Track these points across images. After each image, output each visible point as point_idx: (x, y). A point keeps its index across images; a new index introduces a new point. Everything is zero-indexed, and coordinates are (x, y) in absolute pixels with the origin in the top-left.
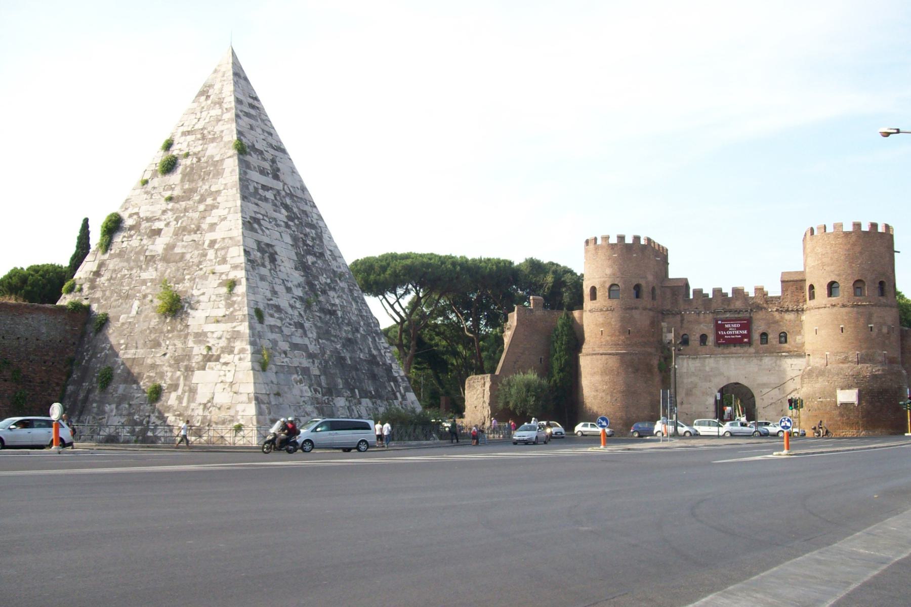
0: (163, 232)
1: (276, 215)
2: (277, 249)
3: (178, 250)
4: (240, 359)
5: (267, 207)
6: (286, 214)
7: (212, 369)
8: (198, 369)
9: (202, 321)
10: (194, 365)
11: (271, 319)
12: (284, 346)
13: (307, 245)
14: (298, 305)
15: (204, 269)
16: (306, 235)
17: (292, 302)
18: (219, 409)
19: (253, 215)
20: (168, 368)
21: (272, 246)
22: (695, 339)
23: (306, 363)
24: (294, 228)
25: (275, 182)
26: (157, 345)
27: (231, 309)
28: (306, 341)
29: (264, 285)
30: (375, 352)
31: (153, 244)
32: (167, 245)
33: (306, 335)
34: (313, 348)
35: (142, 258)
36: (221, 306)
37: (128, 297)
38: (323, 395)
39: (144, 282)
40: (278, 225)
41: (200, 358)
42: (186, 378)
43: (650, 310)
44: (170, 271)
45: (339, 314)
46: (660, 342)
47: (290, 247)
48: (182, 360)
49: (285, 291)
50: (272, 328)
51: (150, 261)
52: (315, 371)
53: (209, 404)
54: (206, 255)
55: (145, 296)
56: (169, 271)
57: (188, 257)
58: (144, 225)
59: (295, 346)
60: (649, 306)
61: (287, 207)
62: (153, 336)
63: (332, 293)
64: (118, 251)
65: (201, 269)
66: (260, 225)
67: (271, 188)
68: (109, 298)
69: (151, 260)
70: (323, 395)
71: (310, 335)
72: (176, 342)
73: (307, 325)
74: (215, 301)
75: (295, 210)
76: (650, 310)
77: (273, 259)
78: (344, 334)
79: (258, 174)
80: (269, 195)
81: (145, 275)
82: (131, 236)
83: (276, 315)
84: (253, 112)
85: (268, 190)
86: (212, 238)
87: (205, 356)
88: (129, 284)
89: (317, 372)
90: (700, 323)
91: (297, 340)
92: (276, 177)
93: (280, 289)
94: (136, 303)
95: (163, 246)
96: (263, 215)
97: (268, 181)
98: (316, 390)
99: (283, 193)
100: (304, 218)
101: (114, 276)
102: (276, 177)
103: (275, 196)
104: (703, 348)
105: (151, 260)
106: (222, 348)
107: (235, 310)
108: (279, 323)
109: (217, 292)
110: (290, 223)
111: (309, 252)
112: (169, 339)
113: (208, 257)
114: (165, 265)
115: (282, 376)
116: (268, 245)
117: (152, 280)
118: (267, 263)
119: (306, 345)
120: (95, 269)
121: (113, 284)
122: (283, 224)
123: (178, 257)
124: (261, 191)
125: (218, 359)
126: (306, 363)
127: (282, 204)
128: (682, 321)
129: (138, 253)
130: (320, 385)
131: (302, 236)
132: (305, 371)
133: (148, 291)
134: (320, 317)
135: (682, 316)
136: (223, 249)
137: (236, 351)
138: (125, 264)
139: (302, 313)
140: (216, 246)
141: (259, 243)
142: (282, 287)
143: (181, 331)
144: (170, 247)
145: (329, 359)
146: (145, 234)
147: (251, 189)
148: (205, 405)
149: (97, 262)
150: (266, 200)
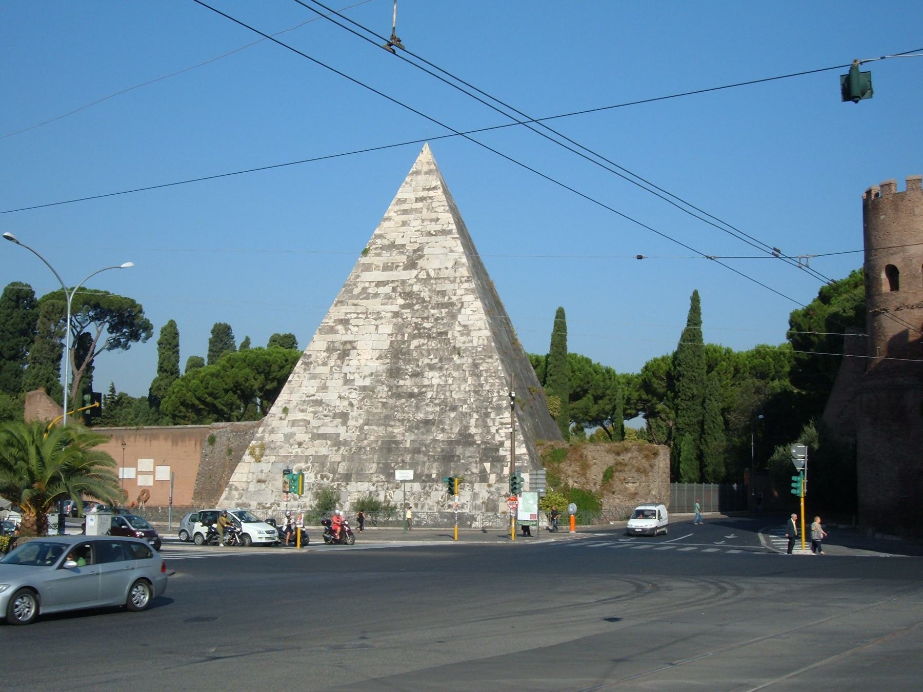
16: (427, 318)
21: (351, 342)
30: (473, 430)
38: (333, 481)
45: (429, 395)
50: (294, 423)
61: (408, 295)
63: (431, 374)
67: (393, 281)
70: (333, 481)
71: (351, 423)
73: (354, 413)
78: (421, 416)
80: (388, 289)
83: (311, 409)
84: (420, 205)
89: (338, 459)
93: (336, 385)
98: (322, 477)
108: (309, 417)
119: (338, 435)
126: (323, 451)
130: (334, 472)
139: (355, 402)
145: (369, 445)
147: (356, 291)
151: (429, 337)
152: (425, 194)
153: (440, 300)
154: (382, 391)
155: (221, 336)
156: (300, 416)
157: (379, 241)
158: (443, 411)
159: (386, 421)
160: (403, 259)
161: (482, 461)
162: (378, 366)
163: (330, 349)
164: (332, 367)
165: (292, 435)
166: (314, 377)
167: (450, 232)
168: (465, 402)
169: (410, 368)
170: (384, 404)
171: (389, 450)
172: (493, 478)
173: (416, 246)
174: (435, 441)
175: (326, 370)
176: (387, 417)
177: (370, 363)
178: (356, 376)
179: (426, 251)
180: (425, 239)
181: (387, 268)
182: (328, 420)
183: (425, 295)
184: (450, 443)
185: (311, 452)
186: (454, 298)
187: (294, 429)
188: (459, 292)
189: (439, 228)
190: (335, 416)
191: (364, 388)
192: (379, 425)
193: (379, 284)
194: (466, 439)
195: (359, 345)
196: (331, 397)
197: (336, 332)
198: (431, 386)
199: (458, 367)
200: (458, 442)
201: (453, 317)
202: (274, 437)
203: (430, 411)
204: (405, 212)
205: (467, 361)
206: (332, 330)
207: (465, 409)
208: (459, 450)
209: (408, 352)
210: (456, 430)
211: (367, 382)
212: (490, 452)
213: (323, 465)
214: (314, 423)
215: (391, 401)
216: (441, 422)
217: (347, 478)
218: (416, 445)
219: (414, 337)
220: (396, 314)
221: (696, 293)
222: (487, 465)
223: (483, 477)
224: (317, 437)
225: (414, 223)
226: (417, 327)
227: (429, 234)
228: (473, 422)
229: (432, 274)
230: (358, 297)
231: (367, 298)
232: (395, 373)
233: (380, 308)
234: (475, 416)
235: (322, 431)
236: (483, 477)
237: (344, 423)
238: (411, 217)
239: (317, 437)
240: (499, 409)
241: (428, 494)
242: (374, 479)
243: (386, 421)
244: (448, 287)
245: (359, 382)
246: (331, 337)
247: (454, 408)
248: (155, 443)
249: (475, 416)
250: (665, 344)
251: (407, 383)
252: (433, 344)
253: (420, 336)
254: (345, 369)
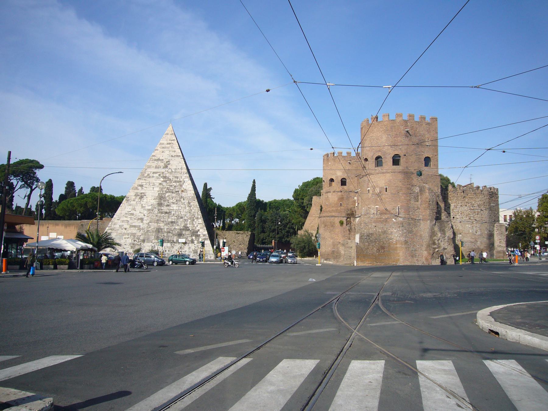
19: (141, 184)
30: (188, 225)
45: (173, 213)
50: (123, 221)
61: (165, 177)
63: (173, 205)
71: (144, 222)
73: (145, 218)
78: (170, 220)
80: (157, 175)
84: (168, 146)
93: (139, 208)
108: (129, 219)
126: (134, 231)
132: (134, 235)
134: (156, 216)
147: (146, 175)
150: (153, 177)
151: (172, 193)
152: (170, 142)
153: (176, 180)
154: (156, 211)
155: (70, 185)
156: (126, 219)
157: (154, 158)
158: (178, 219)
159: (158, 221)
160: (162, 165)
161: (192, 236)
162: (155, 202)
163: (136, 195)
165: (123, 225)
166: (130, 205)
167: (180, 156)
168: (186, 215)
169: (166, 203)
170: (156, 216)
171: (159, 232)
172: (196, 242)
173: (167, 160)
174: (175, 229)
175: (134, 203)
176: (158, 220)
177: (151, 201)
178: (146, 205)
179: (171, 162)
180: (171, 158)
181: (156, 167)
182: (136, 220)
183: (171, 177)
184: (181, 229)
185: (130, 232)
186: (181, 180)
187: (123, 224)
188: (183, 177)
189: (175, 154)
190: (138, 219)
191: (149, 210)
192: (154, 223)
193: (154, 173)
194: (186, 228)
195: (147, 194)
196: (137, 213)
197: (138, 189)
198: (173, 210)
199: (183, 204)
200: (183, 229)
201: (181, 186)
202: (115, 226)
203: (173, 219)
204: (163, 148)
205: (186, 202)
206: (137, 189)
207: (186, 218)
208: (184, 232)
209: (165, 198)
210: (183, 225)
211: (150, 208)
212: (195, 233)
213: (134, 236)
214: (131, 221)
215: (159, 215)
216: (177, 222)
217: (144, 241)
218: (168, 230)
219: (167, 192)
220: (160, 184)
221: (254, 180)
222: (194, 238)
223: (192, 242)
224: (131, 226)
225: (166, 152)
226: (168, 188)
227: (172, 156)
228: (188, 223)
229: (173, 170)
230: (146, 177)
231: (150, 178)
232: (160, 204)
233: (154, 181)
234: (189, 221)
235: (134, 224)
236: (192, 242)
237: (142, 222)
238: (165, 150)
239: (131, 226)
240: (197, 218)
241: (173, 247)
242: (153, 241)
243: (158, 221)
244: (179, 175)
245: (147, 208)
246: (136, 191)
247: (182, 218)
248: (57, 227)
250: (243, 198)
251: (165, 209)
252: (174, 195)
253: (169, 192)
254: (142, 203)
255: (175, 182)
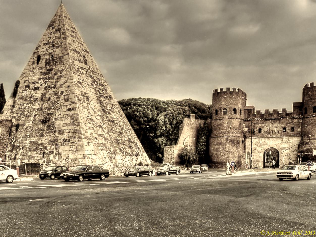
0: (40, 88)
1: (87, 80)
2: (89, 95)
3: (47, 96)
4: (78, 141)
5: (84, 77)
6: (91, 80)
7: (67, 145)
8: (61, 145)
9: (61, 125)
10: (59, 143)
11: (89, 124)
12: (95, 135)
13: (101, 93)
14: (99, 118)
15: (60, 104)
16: (100, 89)
17: (97, 117)
18: (72, 161)
20: (48, 145)
21: (87, 94)
22: (257, 130)
23: (104, 142)
24: (95, 86)
25: (86, 66)
26: (42, 135)
27: (73, 120)
28: (103, 133)
29: (85, 110)
30: (130, 137)
31: (36, 93)
32: (42, 94)
33: (103, 131)
34: (107, 136)
35: (32, 99)
36: (68, 119)
37: (27, 116)
39: (34, 109)
40: (88, 85)
41: (62, 141)
42: (56, 149)
43: (239, 119)
44: (45, 105)
46: (243, 132)
47: (94, 94)
48: (54, 142)
49: (94, 113)
51: (36, 100)
52: (108, 145)
53: (67, 159)
54: (60, 98)
55: (35, 115)
56: (44, 105)
57: (52, 99)
58: (32, 86)
59: (100, 135)
60: (239, 118)
61: (91, 76)
62: (41, 132)
64: (21, 97)
65: (58, 104)
66: (81, 85)
67: (84, 69)
68: (20, 116)
69: (36, 100)
72: (51, 134)
74: (65, 117)
75: (95, 78)
76: (239, 119)
77: (88, 100)
79: (78, 62)
80: (84, 71)
81: (34, 107)
82: (26, 90)
83: (91, 122)
85: (83, 69)
86: (62, 91)
87: (64, 140)
88: (28, 111)
90: (258, 124)
91: (100, 133)
92: (86, 64)
93: (92, 112)
94: (32, 119)
95: (40, 94)
96: (82, 80)
97: (83, 65)
98: (109, 153)
99: (89, 71)
100: (99, 82)
101: (21, 107)
102: (86, 64)
103: (86, 72)
104: (260, 134)
105: (36, 100)
106: (70, 136)
107: (74, 121)
108: (92, 126)
109: (66, 114)
110: (93, 84)
111: (101, 96)
112: (47, 133)
113: (61, 99)
114: (42, 102)
115: (95, 147)
116: (85, 93)
117: (38, 109)
118: (86, 101)
120: (12, 104)
121: (21, 111)
122: (90, 84)
123: (47, 99)
124: (80, 70)
125: (69, 141)
126: (104, 142)
127: (89, 75)
128: (252, 123)
129: (31, 97)
131: (99, 89)
132: (104, 145)
133: (36, 113)
135: (252, 121)
136: (67, 95)
137: (77, 137)
138: (26, 102)
139: (101, 122)
140: (64, 94)
141: (82, 92)
142: (93, 111)
143: (52, 130)
144: (43, 95)
146: (32, 89)
148: (65, 159)
149: (13, 101)
164: (87, 104)
185: (100, 142)
215: (109, 123)
249: (128, 132)
255: (100, 84)
